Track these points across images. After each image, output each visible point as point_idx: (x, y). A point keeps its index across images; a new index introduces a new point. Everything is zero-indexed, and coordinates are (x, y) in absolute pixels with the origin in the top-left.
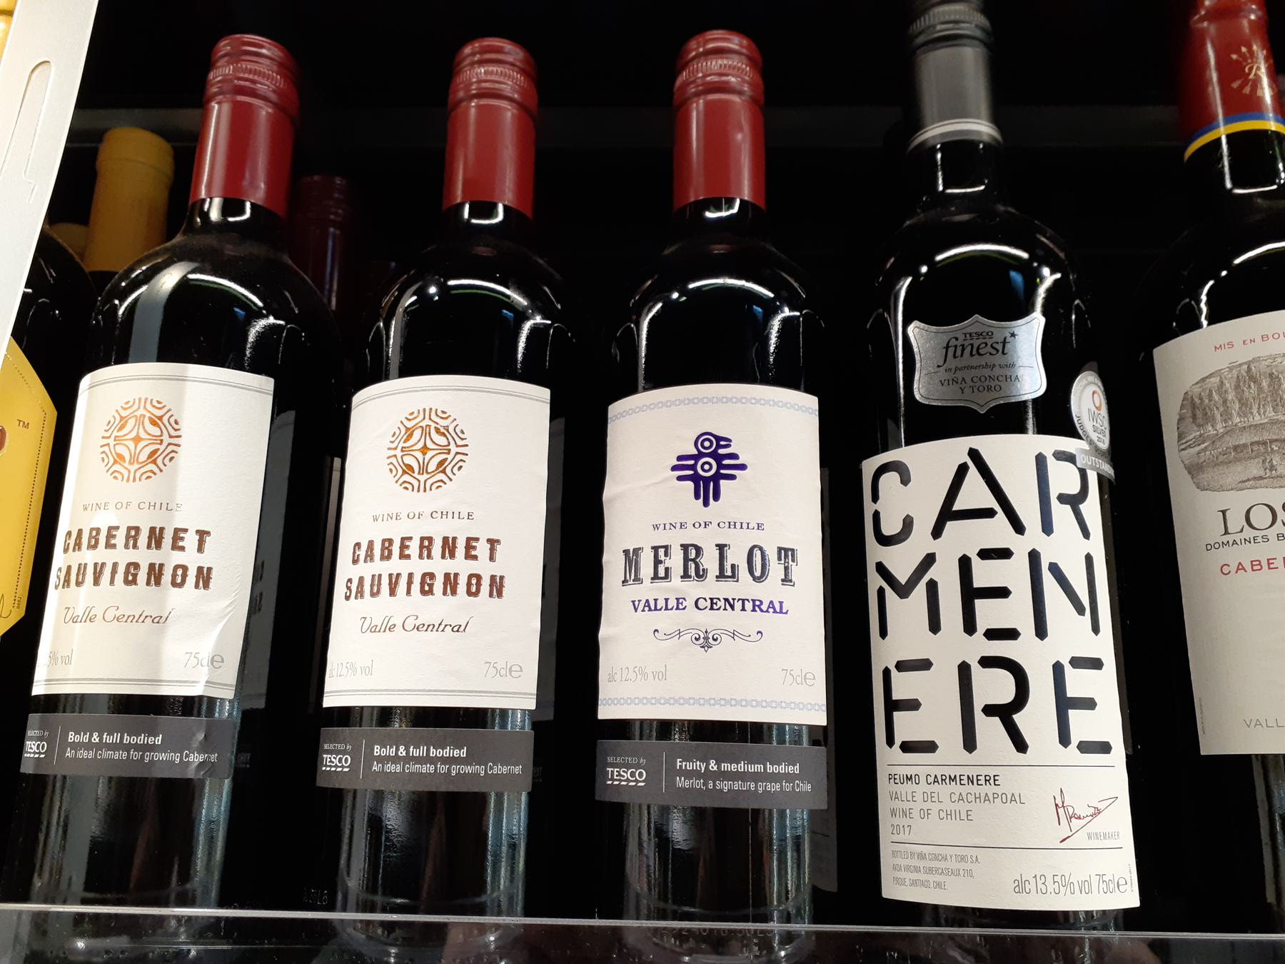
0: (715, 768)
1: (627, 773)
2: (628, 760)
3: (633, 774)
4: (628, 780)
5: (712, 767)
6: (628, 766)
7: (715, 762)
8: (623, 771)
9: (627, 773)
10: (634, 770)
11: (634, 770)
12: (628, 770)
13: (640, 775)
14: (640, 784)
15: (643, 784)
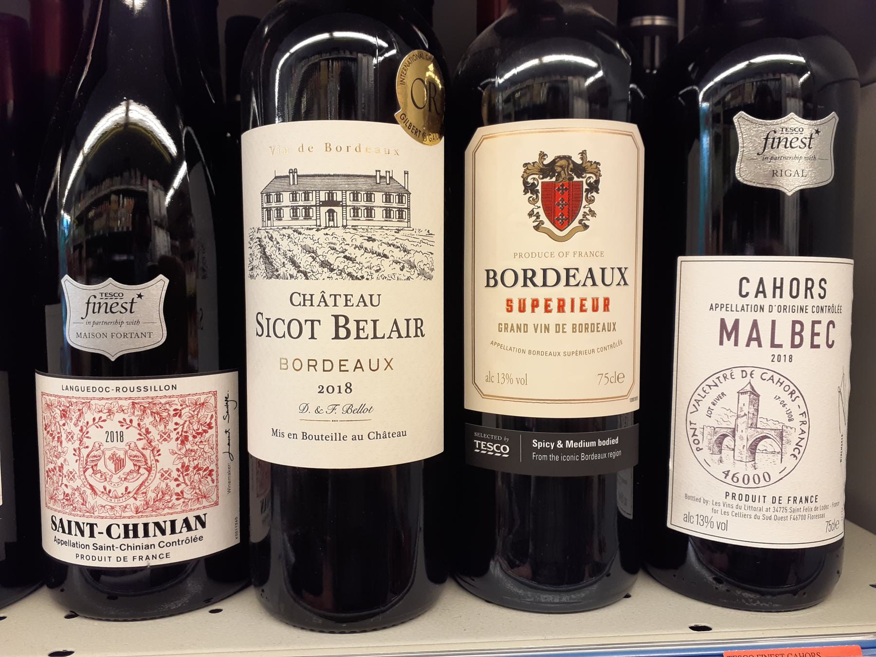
0: (561, 446)
1: (493, 446)
2: (493, 437)
3: (498, 448)
4: (493, 451)
5: (559, 446)
6: (494, 442)
7: (561, 442)
8: (489, 445)
9: (493, 446)
10: (499, 445)
11: (499, 445)
12: (494, 444)
13: (505, 449)
14: (504, 456)
15: (507, 456)
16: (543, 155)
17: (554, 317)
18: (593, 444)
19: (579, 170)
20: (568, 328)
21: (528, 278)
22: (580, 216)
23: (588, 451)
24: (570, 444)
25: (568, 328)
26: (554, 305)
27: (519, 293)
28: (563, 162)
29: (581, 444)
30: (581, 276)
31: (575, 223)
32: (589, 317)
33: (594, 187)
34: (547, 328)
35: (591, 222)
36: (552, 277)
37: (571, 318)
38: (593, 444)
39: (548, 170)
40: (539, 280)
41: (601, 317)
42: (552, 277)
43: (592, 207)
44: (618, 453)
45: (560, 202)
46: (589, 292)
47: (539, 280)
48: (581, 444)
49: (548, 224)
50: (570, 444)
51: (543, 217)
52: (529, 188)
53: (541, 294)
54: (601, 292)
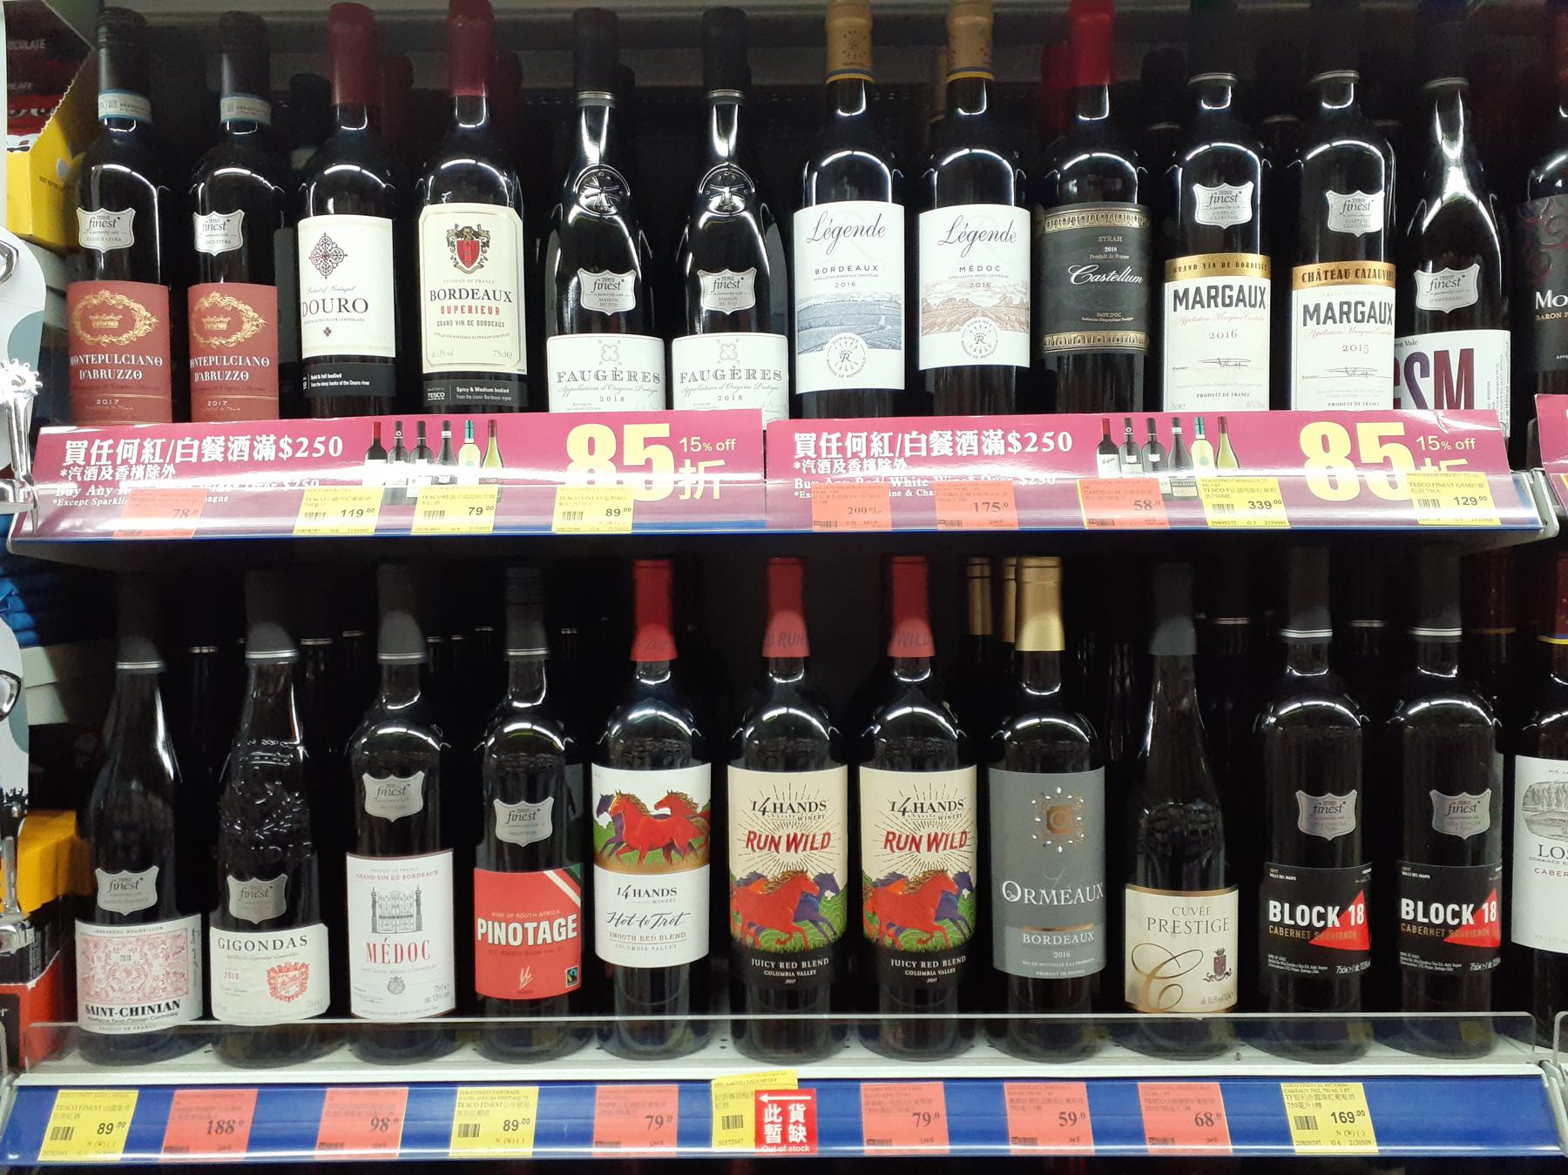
16: (456, 226)
17: (467, 317)
18: (492, 390)
19: (477, 234)
20: (475, 323)
21: (452, 295)
22: (478, 260)
23: (488, 394)
24: (477, 389)
25: (475, 323)
26: (466, 310)
27: (448, 302)
28: (468, 230)
29: (484, 390)
30: (481, 293)
31: (476, 264)
32: (487, 317)
33: (486, 244)
34: (463, 323)
35: (485, 263)
36: (464, 294)
37: (475, 317)
38: (492, 390)
39: (460, 234)
40: (457, 295)
41: (493, 318)
42: (464, 294)
43: (486, 255)
44: (509, 399)
45: (468, 253)
46: (486, 303)
47: (457, 295)
48: (484, 390)
49: (461, 264)
50: (477, 389)
51: (458, 260)
52: (450, 244)
53: (459, 303)
54: (493, 303)
